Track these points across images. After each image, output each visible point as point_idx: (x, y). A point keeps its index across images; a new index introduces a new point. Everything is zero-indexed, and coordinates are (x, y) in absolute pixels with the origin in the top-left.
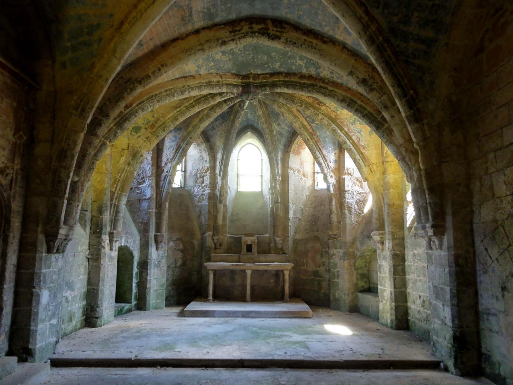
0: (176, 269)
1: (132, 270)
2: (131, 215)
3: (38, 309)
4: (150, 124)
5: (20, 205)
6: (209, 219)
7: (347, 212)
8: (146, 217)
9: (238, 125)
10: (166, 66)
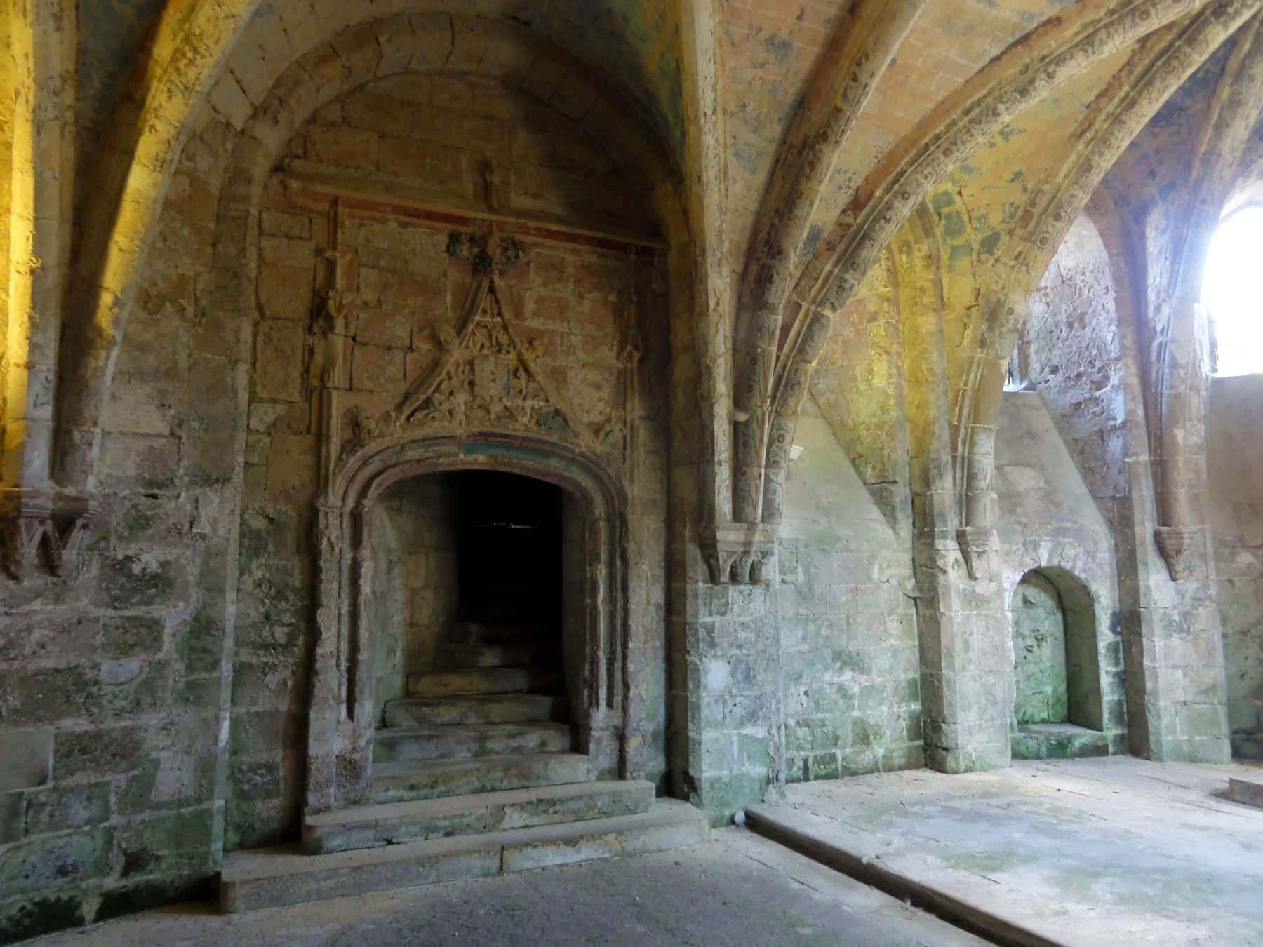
1: (1094, 635)
2: (1085, 478)
3: (699, 698)
4: (1020, 212)
5: (658, 487)
10: (867, 57)
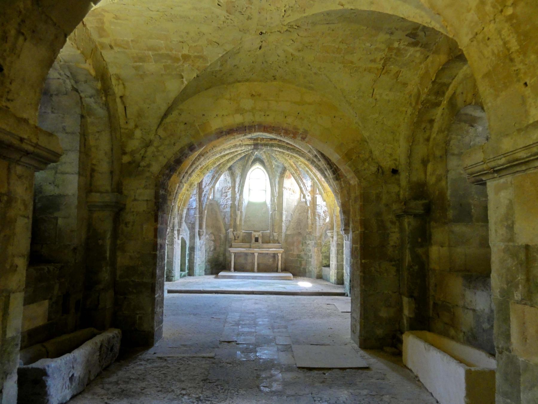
1: (186, 251)
6: (231, 220)
7: (317, 218)
8: (193, 220)
9: (250, 162)
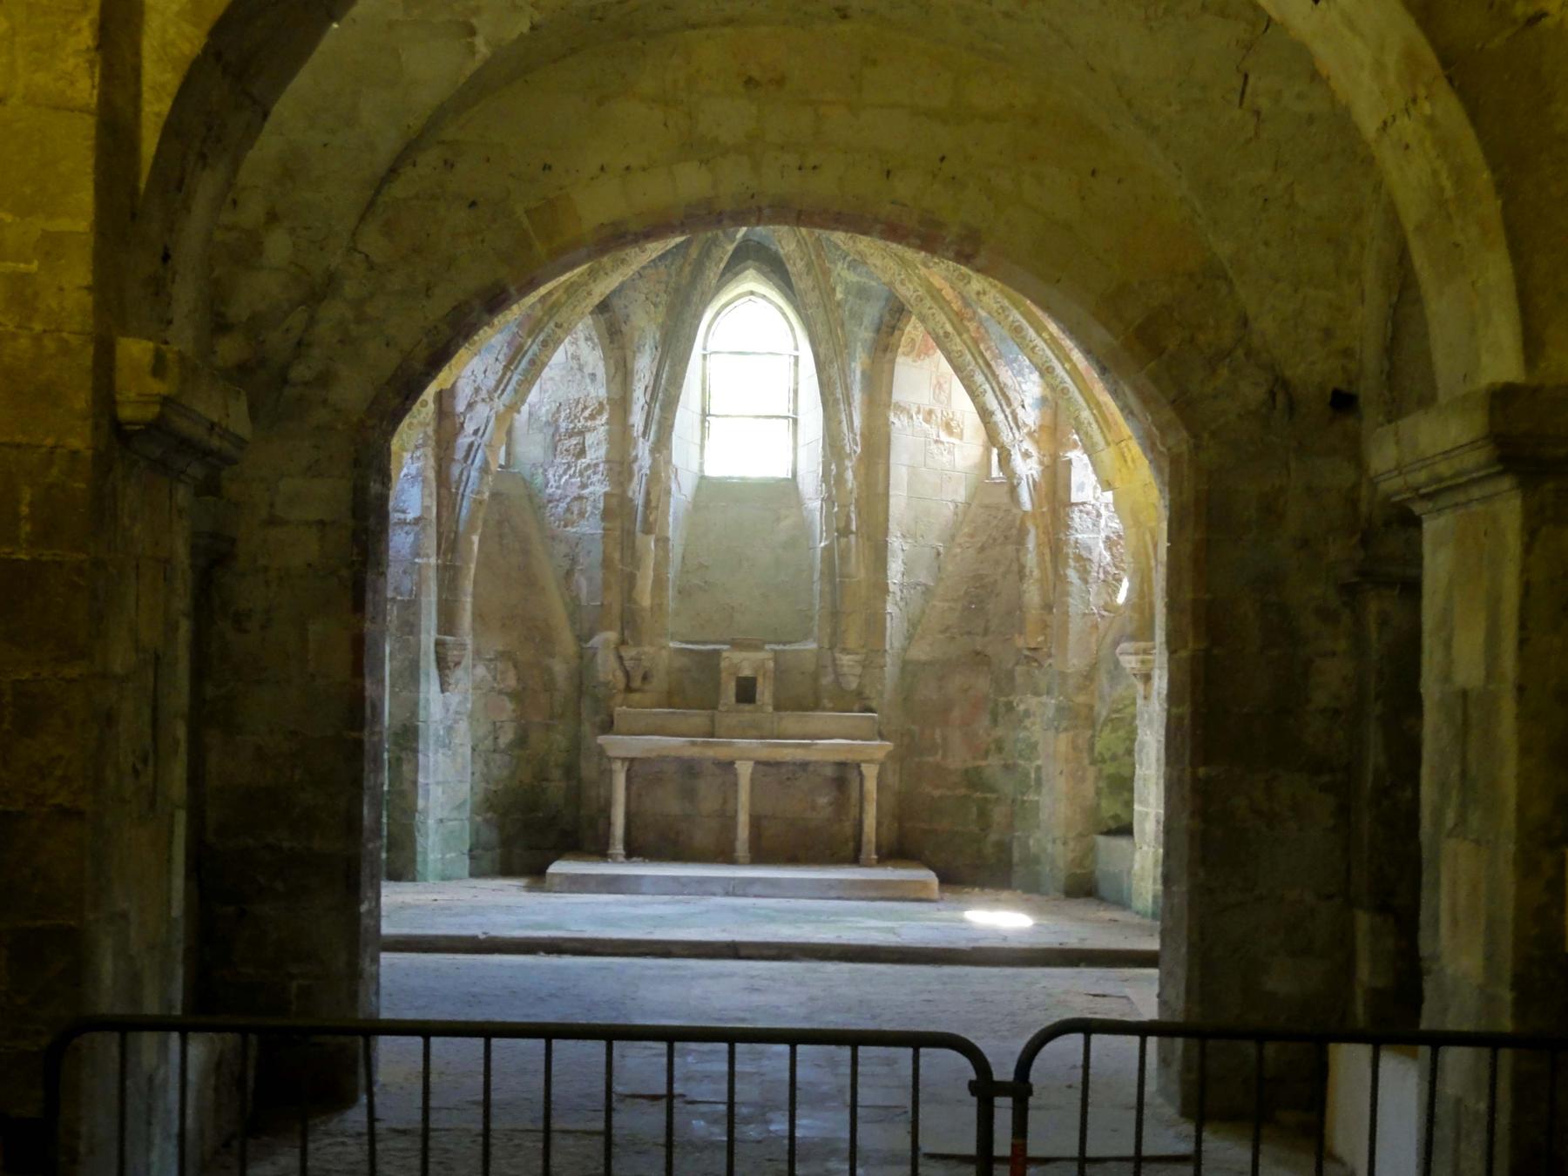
0: (497, 756)
6: (606, 586)
7: (1072, 575)
8: (407, 584)
